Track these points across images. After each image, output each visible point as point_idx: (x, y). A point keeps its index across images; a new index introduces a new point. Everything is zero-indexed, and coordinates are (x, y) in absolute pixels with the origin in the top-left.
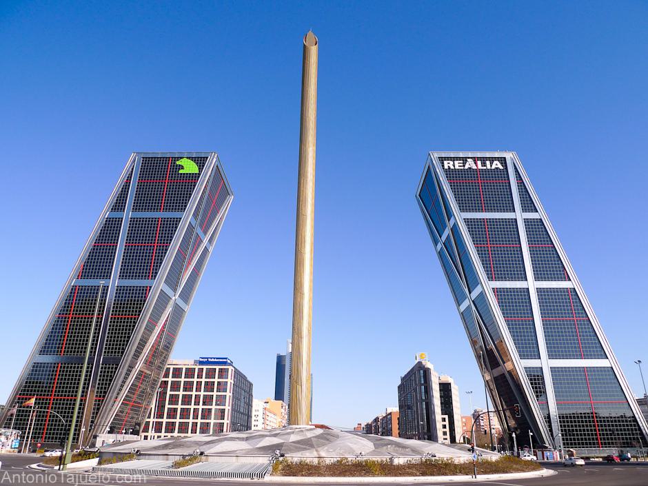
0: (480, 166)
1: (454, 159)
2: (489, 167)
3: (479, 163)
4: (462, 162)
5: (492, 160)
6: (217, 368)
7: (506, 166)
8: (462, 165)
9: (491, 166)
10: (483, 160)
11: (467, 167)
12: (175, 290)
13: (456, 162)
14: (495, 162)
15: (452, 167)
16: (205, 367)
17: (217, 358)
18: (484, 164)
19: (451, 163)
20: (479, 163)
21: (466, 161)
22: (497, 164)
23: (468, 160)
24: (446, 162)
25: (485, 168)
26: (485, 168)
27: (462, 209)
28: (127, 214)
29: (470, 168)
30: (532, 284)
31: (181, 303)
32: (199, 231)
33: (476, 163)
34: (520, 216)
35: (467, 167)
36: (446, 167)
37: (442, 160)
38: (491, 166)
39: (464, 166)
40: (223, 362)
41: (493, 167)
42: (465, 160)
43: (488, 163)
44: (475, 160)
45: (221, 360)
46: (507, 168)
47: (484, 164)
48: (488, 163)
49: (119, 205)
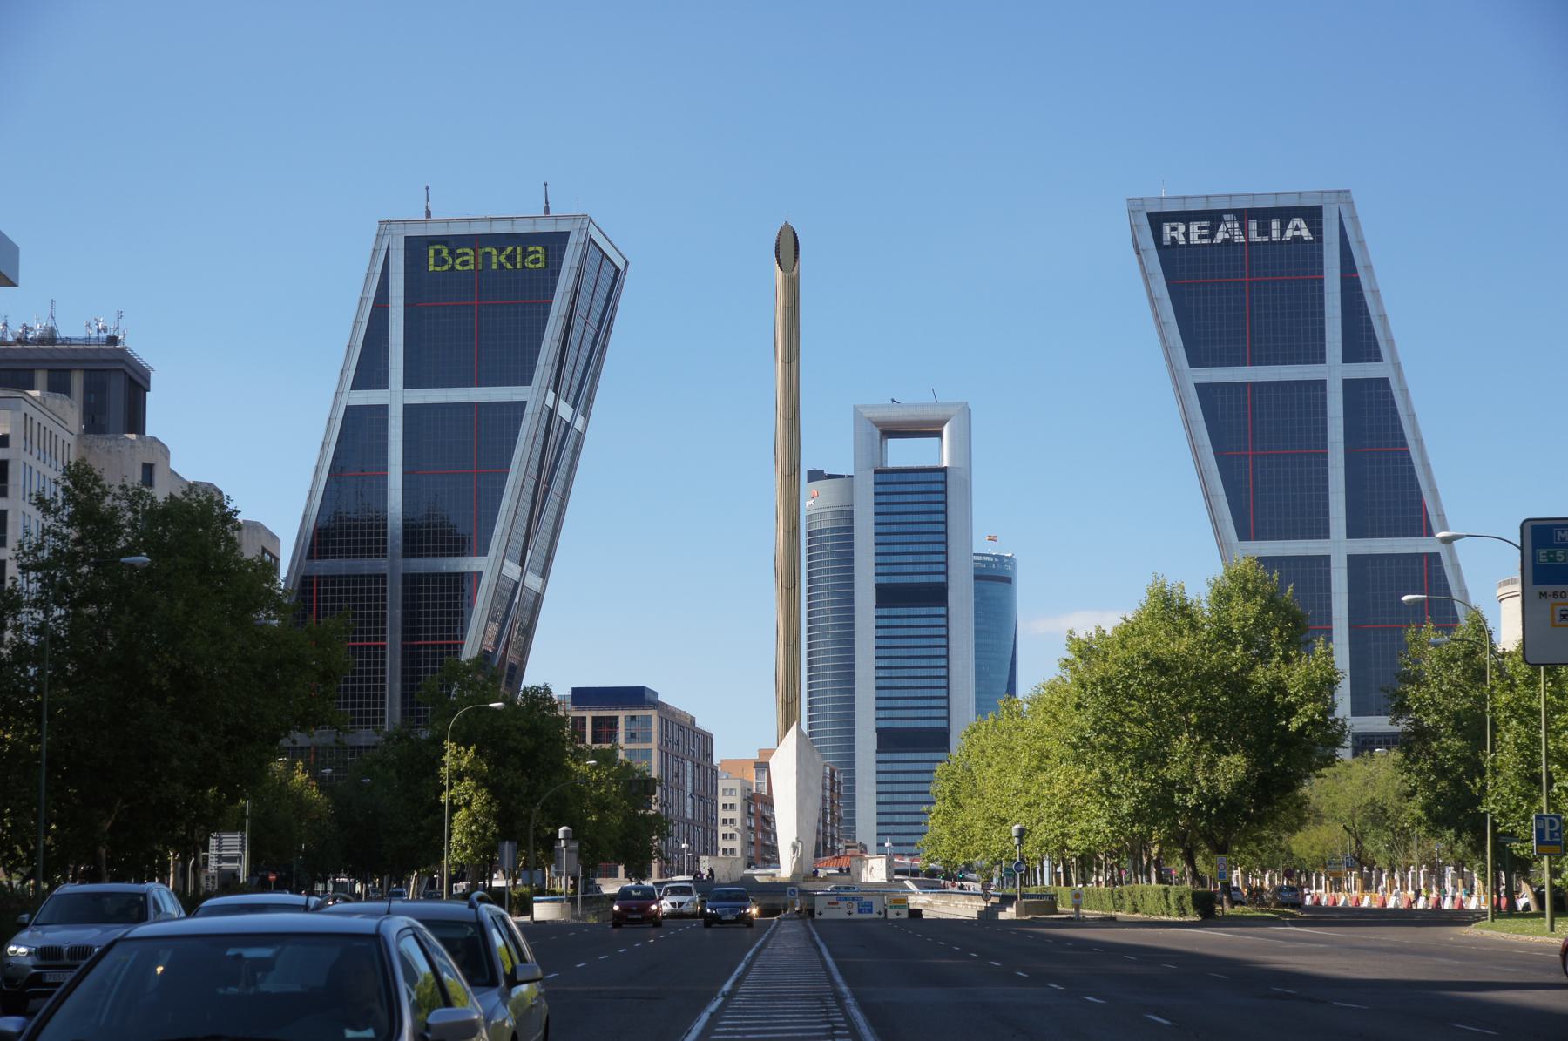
0: (1255, 237)
1: (1186, 217)
2: (1275, 235)
3: (1253, 225)
4: (1205, 224)
5: (1285, 215)
6: (622, 715)
7: (1320, 232)
8: (1205, 232)
9: (1282, 233)
10: (1263, 216)
11: (1220, 236)
12: (522, 565)
13: (1194, 227)
14: (1296, 222)
15: (1181, 240)
16: (589, 715)
18: (1264, 230)
19: (1182, 228)
20: (1253, 225)
21: (1222, 220)
22: (1299, 229)
23: (1226, 217)
24: (1167, 228)
25: (1266, 239)
26: (1266, 239)
27: (1195, 361)
28: (395, 397)
29: (1227, 242)
30: (1338, 547)
31: (533, 581)
32: (565, 411)
33: (1244, 229)
34: (1334, 371)
35: (1220, 236)
36: (1167, 240)
37: (1157, 220)
38: (1282, 233)
39: (1212, 236)
40: (637, 697)
41: (1289, 234)
42: (1213, 218)
43: (1275, 224)
44: (1243, 216)
46: (1320, 240)
47: (1264, 230)
48: (1275, 224)
49: (369, 371)
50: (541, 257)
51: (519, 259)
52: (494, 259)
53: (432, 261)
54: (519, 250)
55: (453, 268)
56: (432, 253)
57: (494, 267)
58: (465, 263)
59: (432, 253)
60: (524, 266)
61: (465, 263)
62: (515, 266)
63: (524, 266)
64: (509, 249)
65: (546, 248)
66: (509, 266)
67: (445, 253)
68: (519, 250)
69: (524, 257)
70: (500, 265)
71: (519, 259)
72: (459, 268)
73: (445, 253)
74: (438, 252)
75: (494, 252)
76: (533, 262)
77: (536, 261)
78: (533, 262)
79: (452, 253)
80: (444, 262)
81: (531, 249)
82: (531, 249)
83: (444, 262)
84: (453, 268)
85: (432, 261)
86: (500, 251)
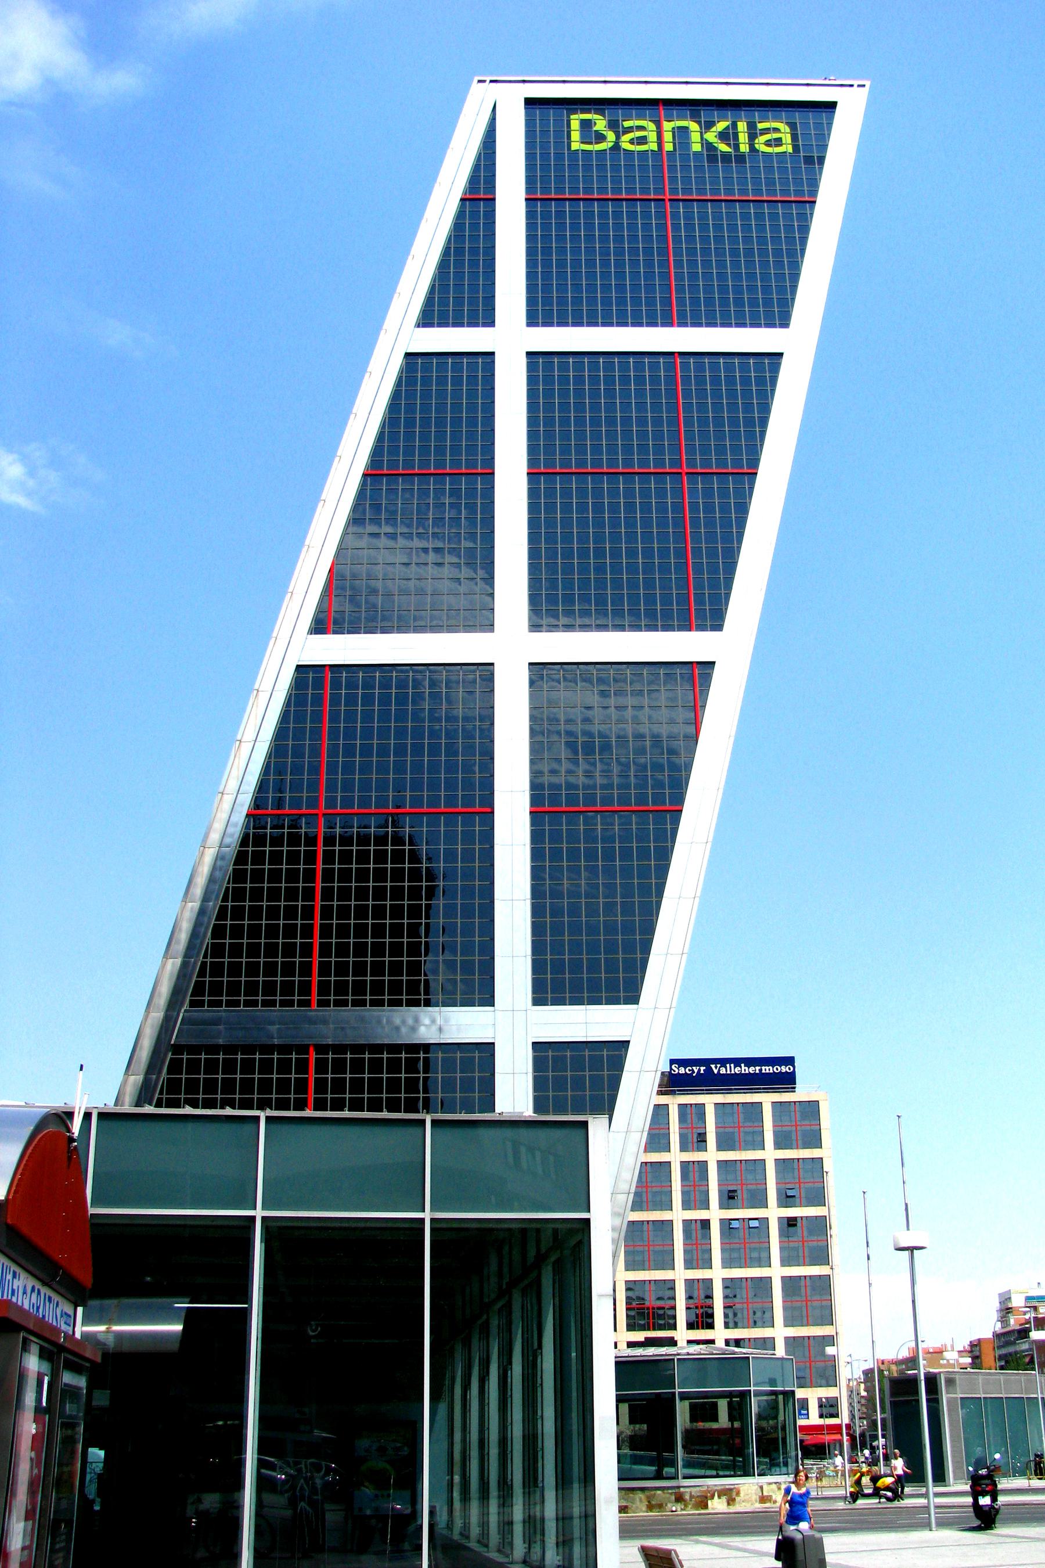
16: (709, 1101)
17: (750, 1062)
45: (767, 1069)
50: (787, 138)
51: (743, 138)
52: (695, 137)
53: (575, 136)
54: (742, 126)
55: (616, 147)
56: (575, 125)
57: (696, 147)
58: (642, 140)
59: (575, 125)
60: (753, 149)
61: (642, 140)
62: (736, 147)
63: (753, 149)
64: (721, 126)
65: (792, 126)
66: (723, 148)
67: (601, 124)
68: (742, 126)
69: (752, 136)
70: (709, 146)
71: (743, 138)
72: (626, 146)
73: (601, 124)
74: (586, 125)
75: (694, 126)
76: (768, 144)
77: (778, 142)
78: (768, 144)
79: (613, 125)
80: (600, 138)
81: (760, 126)
82: (760, 126)
83: (600, 138)
84: (616, 147)
85: (575, 136)
86: (709, 125)
